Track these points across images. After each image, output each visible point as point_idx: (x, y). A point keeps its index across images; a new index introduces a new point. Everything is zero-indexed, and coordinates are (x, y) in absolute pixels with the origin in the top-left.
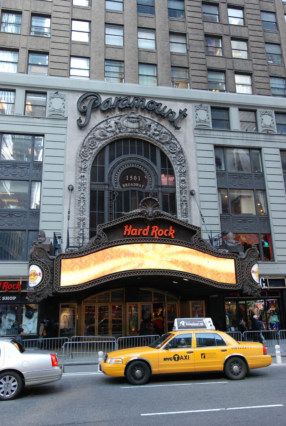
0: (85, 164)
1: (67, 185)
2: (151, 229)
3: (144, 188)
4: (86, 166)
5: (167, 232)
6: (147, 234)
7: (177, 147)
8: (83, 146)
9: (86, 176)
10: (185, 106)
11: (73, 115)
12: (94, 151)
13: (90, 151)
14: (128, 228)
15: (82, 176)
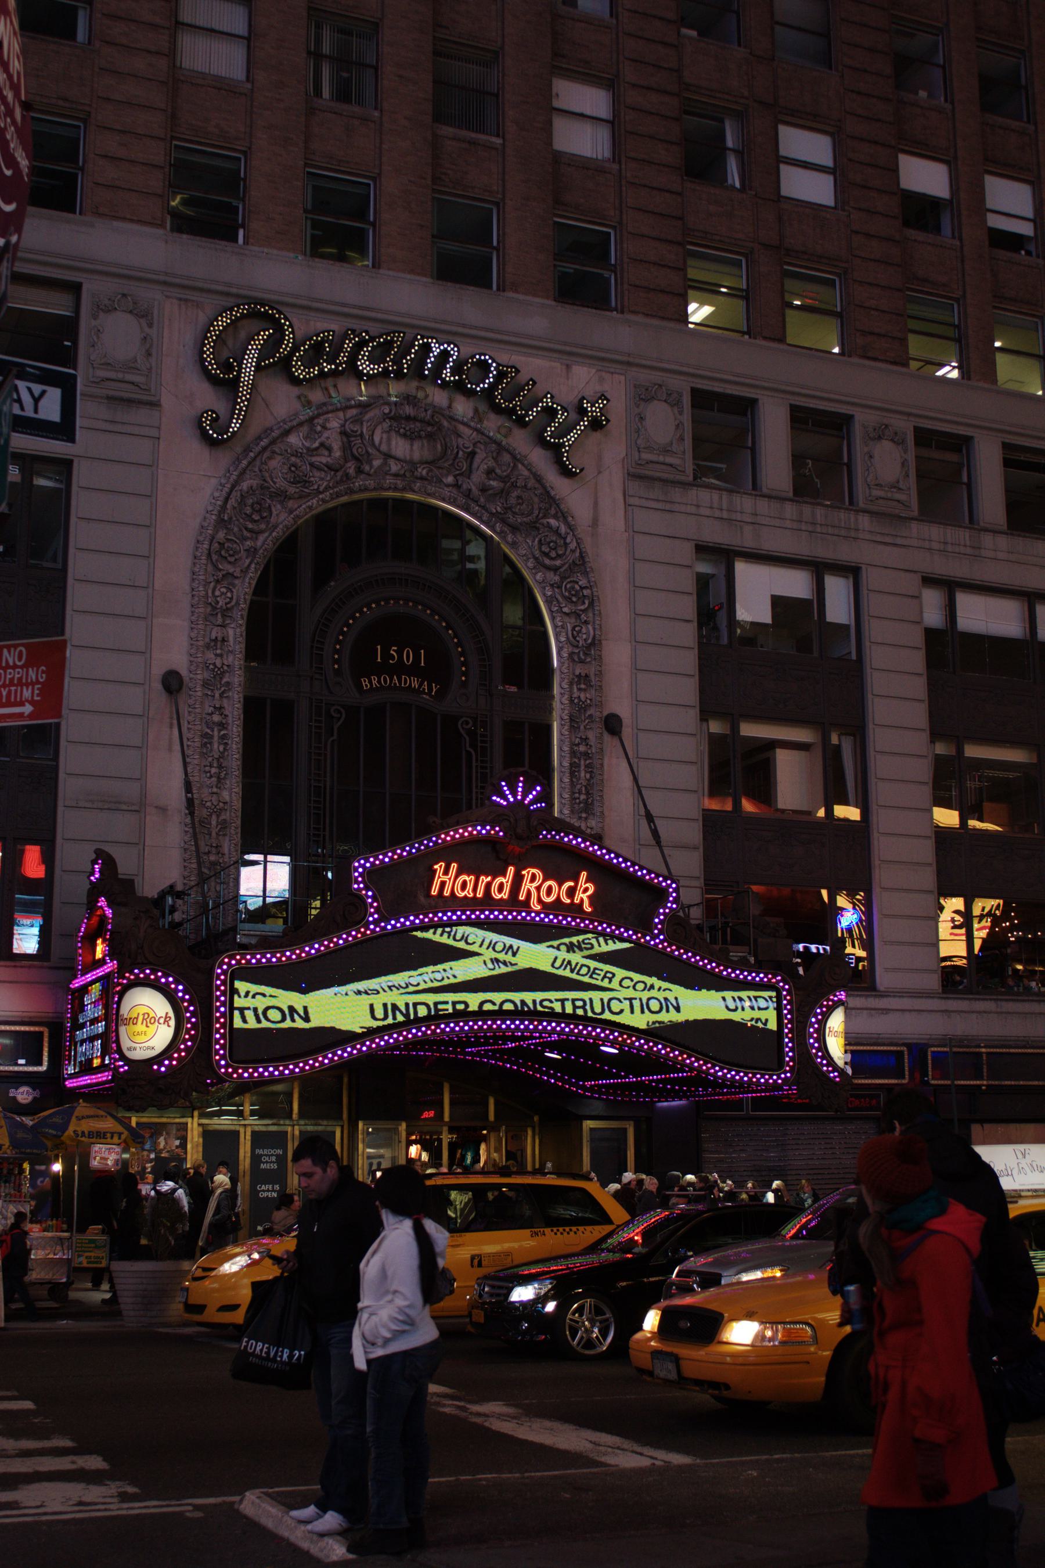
0: (229, 595)
1: (158, 671)
2: (518, 880)
3: (441, 695)
4: (231, 599)
5: (571, 892)
6: (505, 895)
7: (566, 544)
8: (221, 523)
9: (231, 639)
10: (601, 380)
11: (186, 394)
12: (266, 542)
13: (248, 543)
14: (446, 872)
15: (219, 639)
